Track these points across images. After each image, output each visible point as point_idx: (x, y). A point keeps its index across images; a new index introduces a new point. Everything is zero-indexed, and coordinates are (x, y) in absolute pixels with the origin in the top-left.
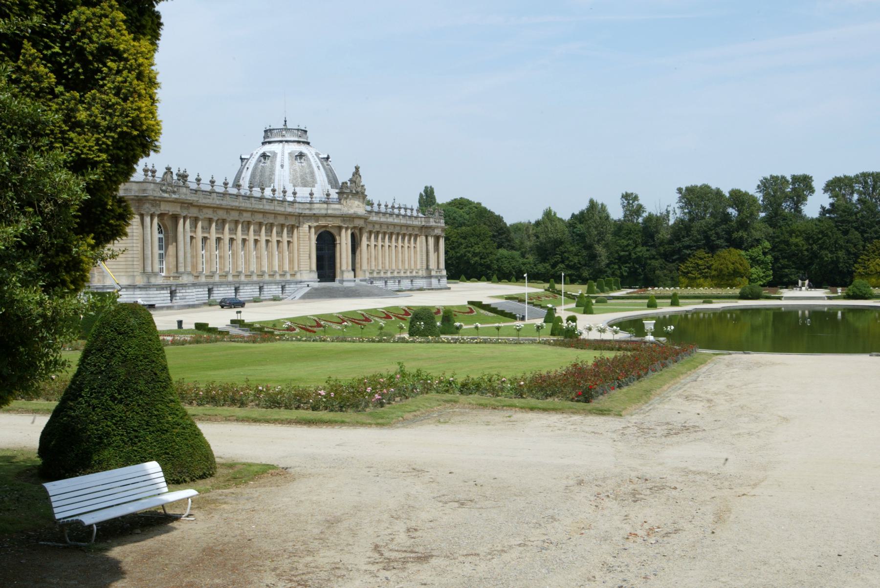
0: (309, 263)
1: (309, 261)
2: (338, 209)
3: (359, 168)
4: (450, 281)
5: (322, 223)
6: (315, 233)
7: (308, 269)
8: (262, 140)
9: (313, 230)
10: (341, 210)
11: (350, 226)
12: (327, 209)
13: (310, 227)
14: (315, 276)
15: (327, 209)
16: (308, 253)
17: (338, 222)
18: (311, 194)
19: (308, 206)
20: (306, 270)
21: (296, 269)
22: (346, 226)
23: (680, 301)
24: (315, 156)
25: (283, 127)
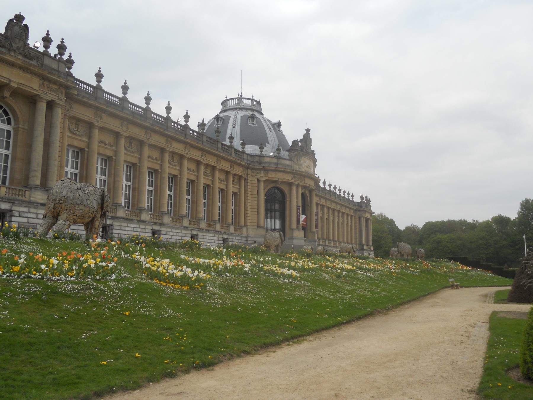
0: (256, 218)
1: (256, 216)
3: (310, 130)
5: (272, 176)
6: (264, 189)
7: (256, 224)
9: (262, 184)
11: (301, 184)
13: (259, 180)
16: (256, 207)
17: (288, 178)
20: (254, 226)
21: (242, 223)
22: (297, 183)
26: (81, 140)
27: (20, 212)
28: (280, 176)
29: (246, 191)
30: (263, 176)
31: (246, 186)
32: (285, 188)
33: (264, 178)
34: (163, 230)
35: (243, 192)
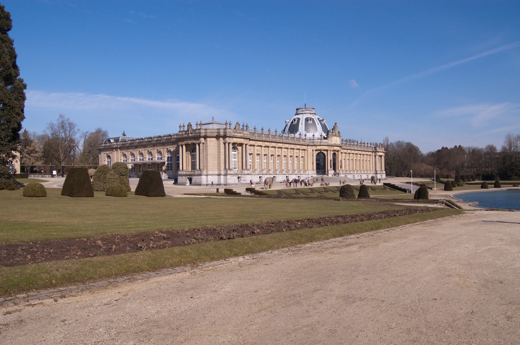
1: (312, 165)
2: (326, 142)
4: (387, 177)
5: (319, 148)
8: (295, 114)
11: (332, 150)
12: (321, 142)
13: (313, 150)
14: (315, 172)
15: (321, 142)
17: (326, 148)
18: (313, 136)
19: (312, 141)
21: (306, 169)
22: (330, 150)
24: (317, 120)
26: (252, 151)
27: (243, 177)
29: (307, 155)
30: (314, 148)
31: (307, 153)
32: (325, 152)
33: (315, 149)
34: (277, 176)
35: (306, 156)
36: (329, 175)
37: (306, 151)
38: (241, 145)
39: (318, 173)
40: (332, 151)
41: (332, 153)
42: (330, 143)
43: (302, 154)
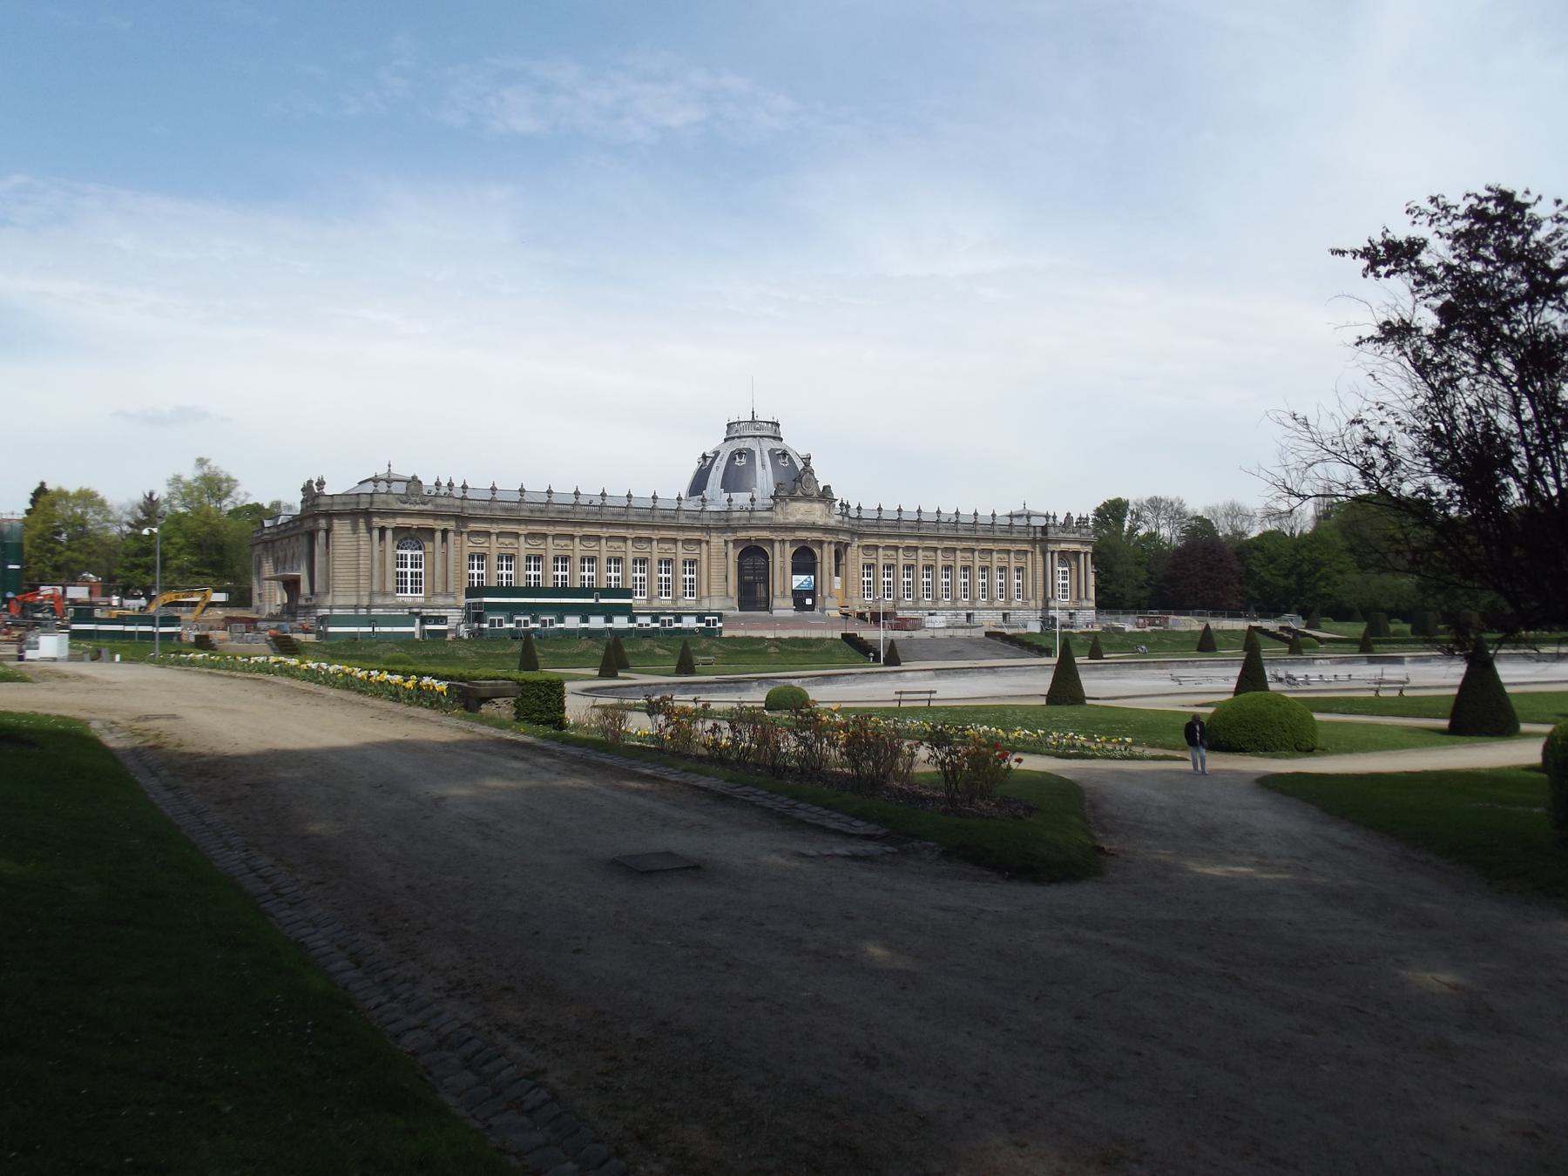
2: (766, 518)
5: (742, 535)
9: (731, 545)
10: (772, 519)
13: (726, 542)
14: (735, 603)
18: (753, 500)
21: (705, 593)
22: (779, 539)
23: (1374, 646)
24: (766, 454)
25: (750, 419)
28: (753, 534)
30: (730, 536)
31: (709, 549)
33: (733, 538)
35: (704, 556)
36: (774, 611)
37: (704, 545)
38: (431, 532)
39: (743, 606)
40: (788, 545)
41: (790, 551)
42: (782, 521)
43: (681, 553)
